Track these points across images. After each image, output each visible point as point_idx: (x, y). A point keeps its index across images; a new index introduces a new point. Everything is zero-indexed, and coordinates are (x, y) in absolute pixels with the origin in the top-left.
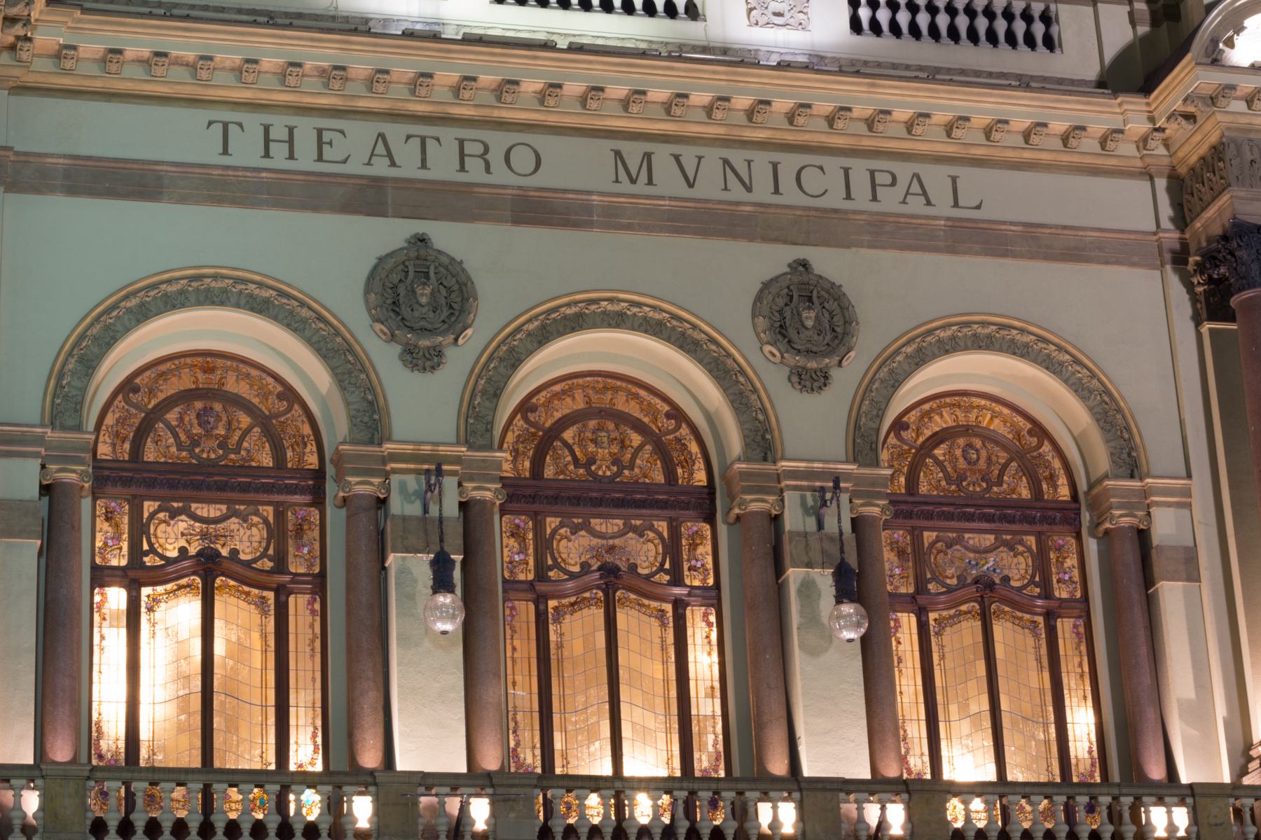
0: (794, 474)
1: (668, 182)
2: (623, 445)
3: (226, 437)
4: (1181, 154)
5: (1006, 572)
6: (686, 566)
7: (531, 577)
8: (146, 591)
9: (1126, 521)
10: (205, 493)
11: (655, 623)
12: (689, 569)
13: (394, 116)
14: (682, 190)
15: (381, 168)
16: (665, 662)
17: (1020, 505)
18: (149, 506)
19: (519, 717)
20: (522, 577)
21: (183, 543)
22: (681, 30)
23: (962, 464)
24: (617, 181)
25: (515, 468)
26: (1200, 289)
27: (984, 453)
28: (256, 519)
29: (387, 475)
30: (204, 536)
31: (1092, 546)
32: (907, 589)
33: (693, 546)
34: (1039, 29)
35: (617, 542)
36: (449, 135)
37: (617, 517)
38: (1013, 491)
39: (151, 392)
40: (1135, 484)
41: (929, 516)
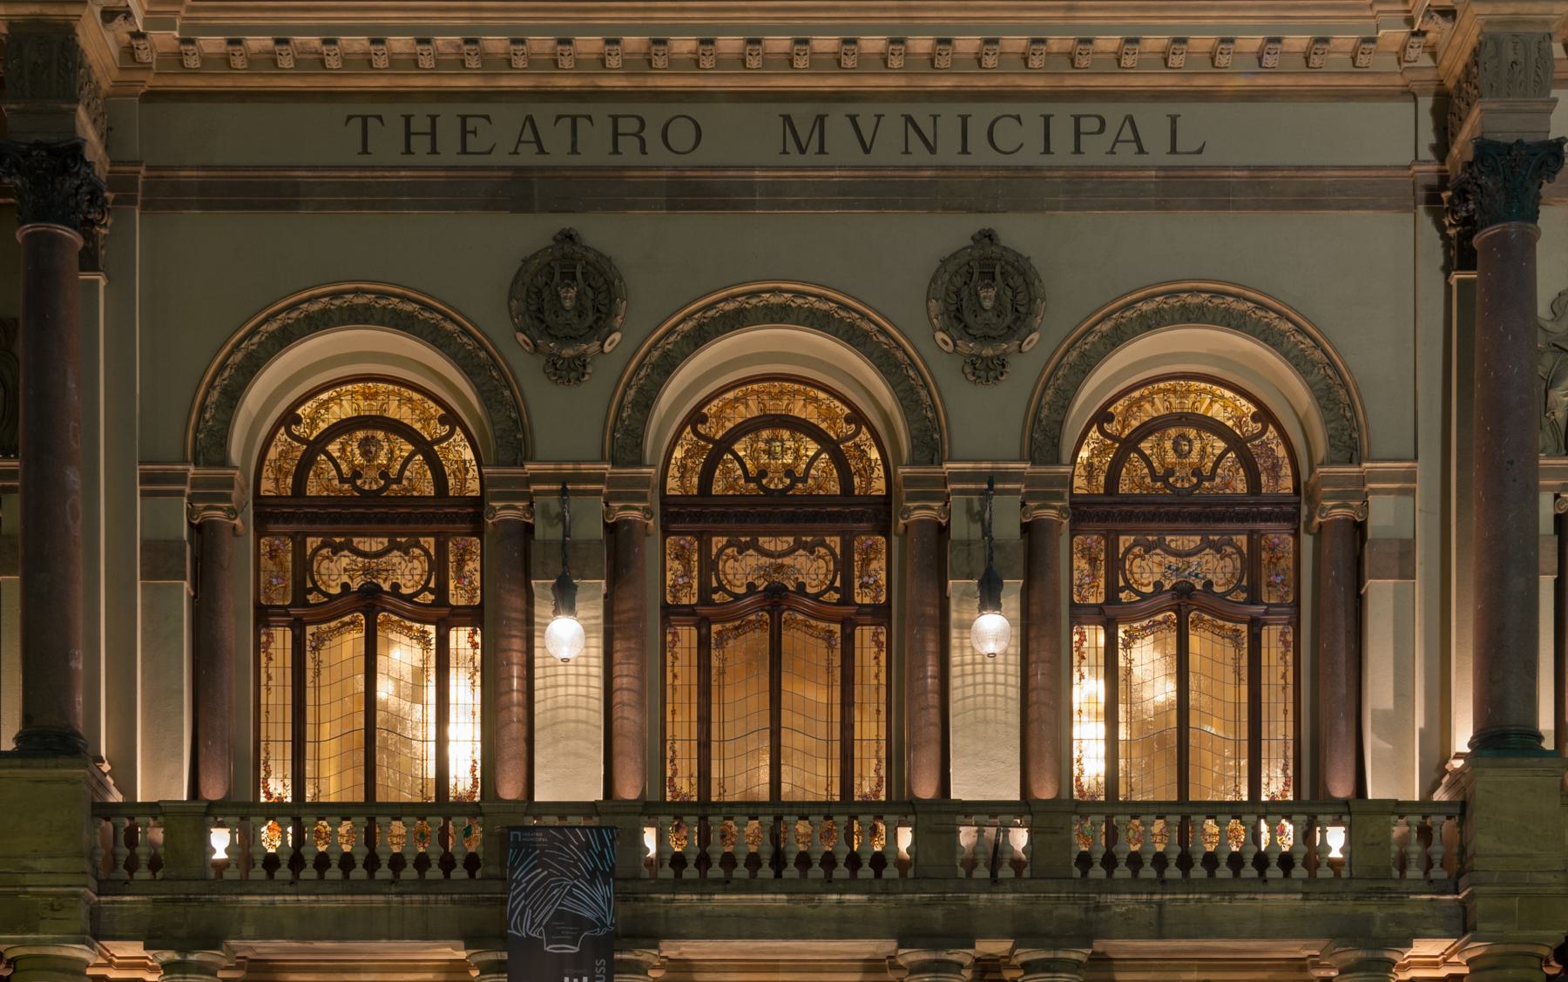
3: (388, 467)
4: (1446, 63)
5: (1209, 576)
7: (694, 600)
8: (310, 629)
10: (364, 527)
11: (822, 644)
12: (861, 587)
16: (830, 686)
19: (677, 746)
20: (685, 601)
21: (345, 579)
24: (785, 152)
25: (683, 486)
26: (1452, 232)
28: (417, 551)
30: (366, 571)
31: (1307, 541)
32: (1096, 597)
38: (1227, 485)
39: (313, 423)
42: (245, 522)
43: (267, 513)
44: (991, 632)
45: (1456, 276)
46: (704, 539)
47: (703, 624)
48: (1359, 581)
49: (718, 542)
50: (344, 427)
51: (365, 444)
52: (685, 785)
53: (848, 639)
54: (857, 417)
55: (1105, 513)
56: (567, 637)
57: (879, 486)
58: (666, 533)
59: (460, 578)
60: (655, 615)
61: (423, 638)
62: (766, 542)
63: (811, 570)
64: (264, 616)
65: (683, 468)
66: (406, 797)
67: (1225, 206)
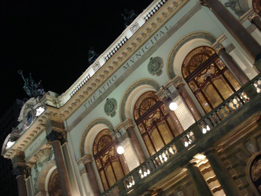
2: (148, 102)
6: (164, 113)
9: (219, 49)
13: (99, 87)
14: (132, 63)
15: (101, 94)
17: (208, 60)
18: (101, 157)
20: (144, 132)
23: (195, 63)
27: (198, 58)
35: (154, 117)
36: (106, 83)
37: (152, 114)
40: (216, 43)
62: (150, 117)
63: (157, 116)
67: (178, 29)
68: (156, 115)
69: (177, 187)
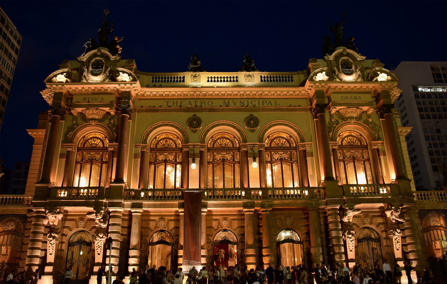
0: (249, 145)
1: (231, 104)
9: (302, 149)
14: (233, 105)
22: (236, 83)
23: (278, 142)
29: (189, 148)
33: (236, 156)
34: (290, 79)
41: (273, 150)
42: (149, 151)
43: (151, 150)
44: (254, 165)
45: (315, 120)
46: (213, 153)
47: (213, 164)
48: (306, 158)
49: (215, 153)
50: (163, 139)
51: (166, 141)
52: (211, 186)
53: (234, 166)
54: (234, 137)
55: (269, 149)
56: (194, 166)
57: (238, 146)
58: (208, 152)
59: (178, 158)
60: (206, 163)
61: (173, 166)
64: (150, 163)
65: (210, 144)
66: (170, 188)
68: (227, 155)
69: (225, 217)
